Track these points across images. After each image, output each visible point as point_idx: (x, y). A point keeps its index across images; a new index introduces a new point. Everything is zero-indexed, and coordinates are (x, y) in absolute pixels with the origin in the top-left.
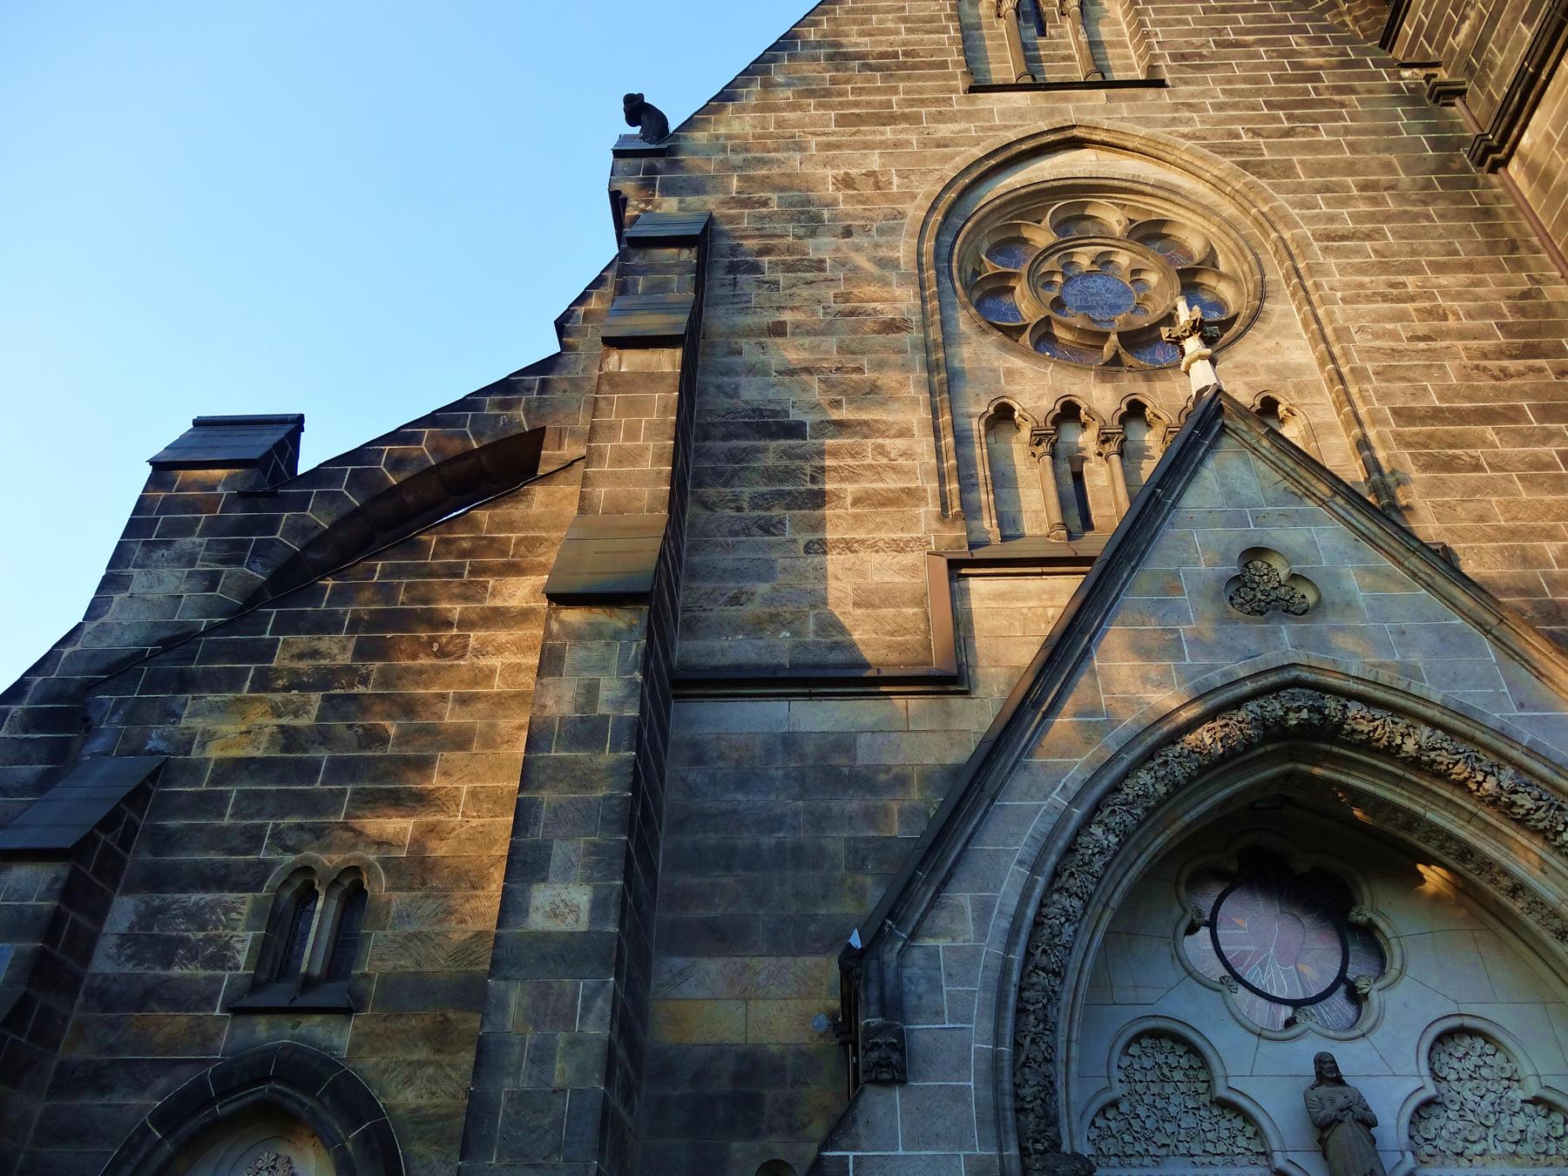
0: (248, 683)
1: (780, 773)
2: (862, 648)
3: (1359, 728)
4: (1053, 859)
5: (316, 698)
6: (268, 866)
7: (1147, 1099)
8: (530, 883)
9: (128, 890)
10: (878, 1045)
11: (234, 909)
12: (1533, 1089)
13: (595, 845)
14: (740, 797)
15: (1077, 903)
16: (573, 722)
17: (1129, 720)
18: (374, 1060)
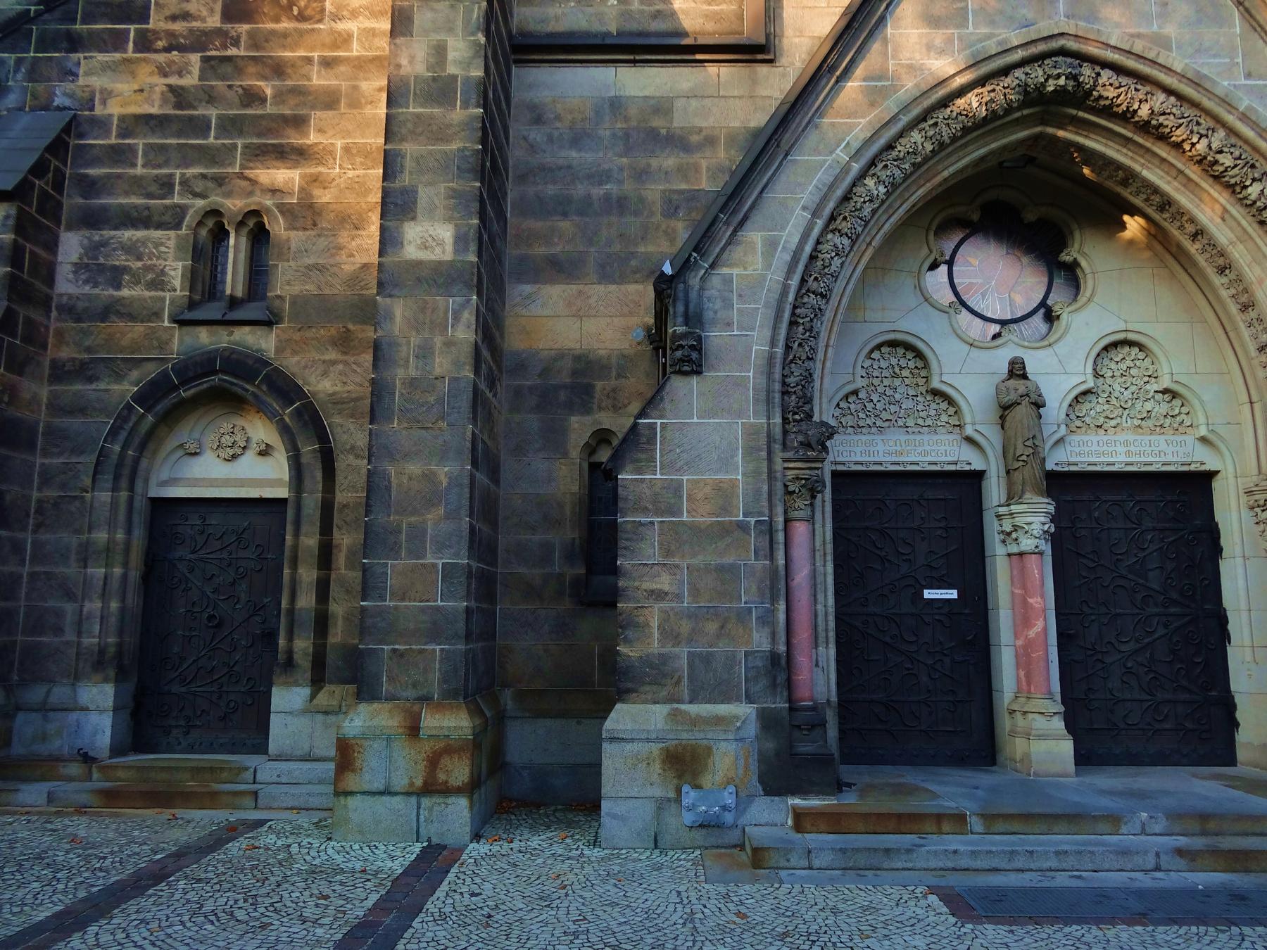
0: (131, 44)
1: (608, 133)
2: (681, 16)
3: (1105, 94)
4: (831, 205)
5: (195, 58)
6: (181, 211)
7: (880, 389)
8: (402, 221)
9: (69, 228)
10: (682, 347)
11: (162, 244)
12: (1166, 383)
13: (453, 190)
14: (574, 154)
15: (846, 241)
16: (425, 80)
17: (909, 86)
18: (296, 359)
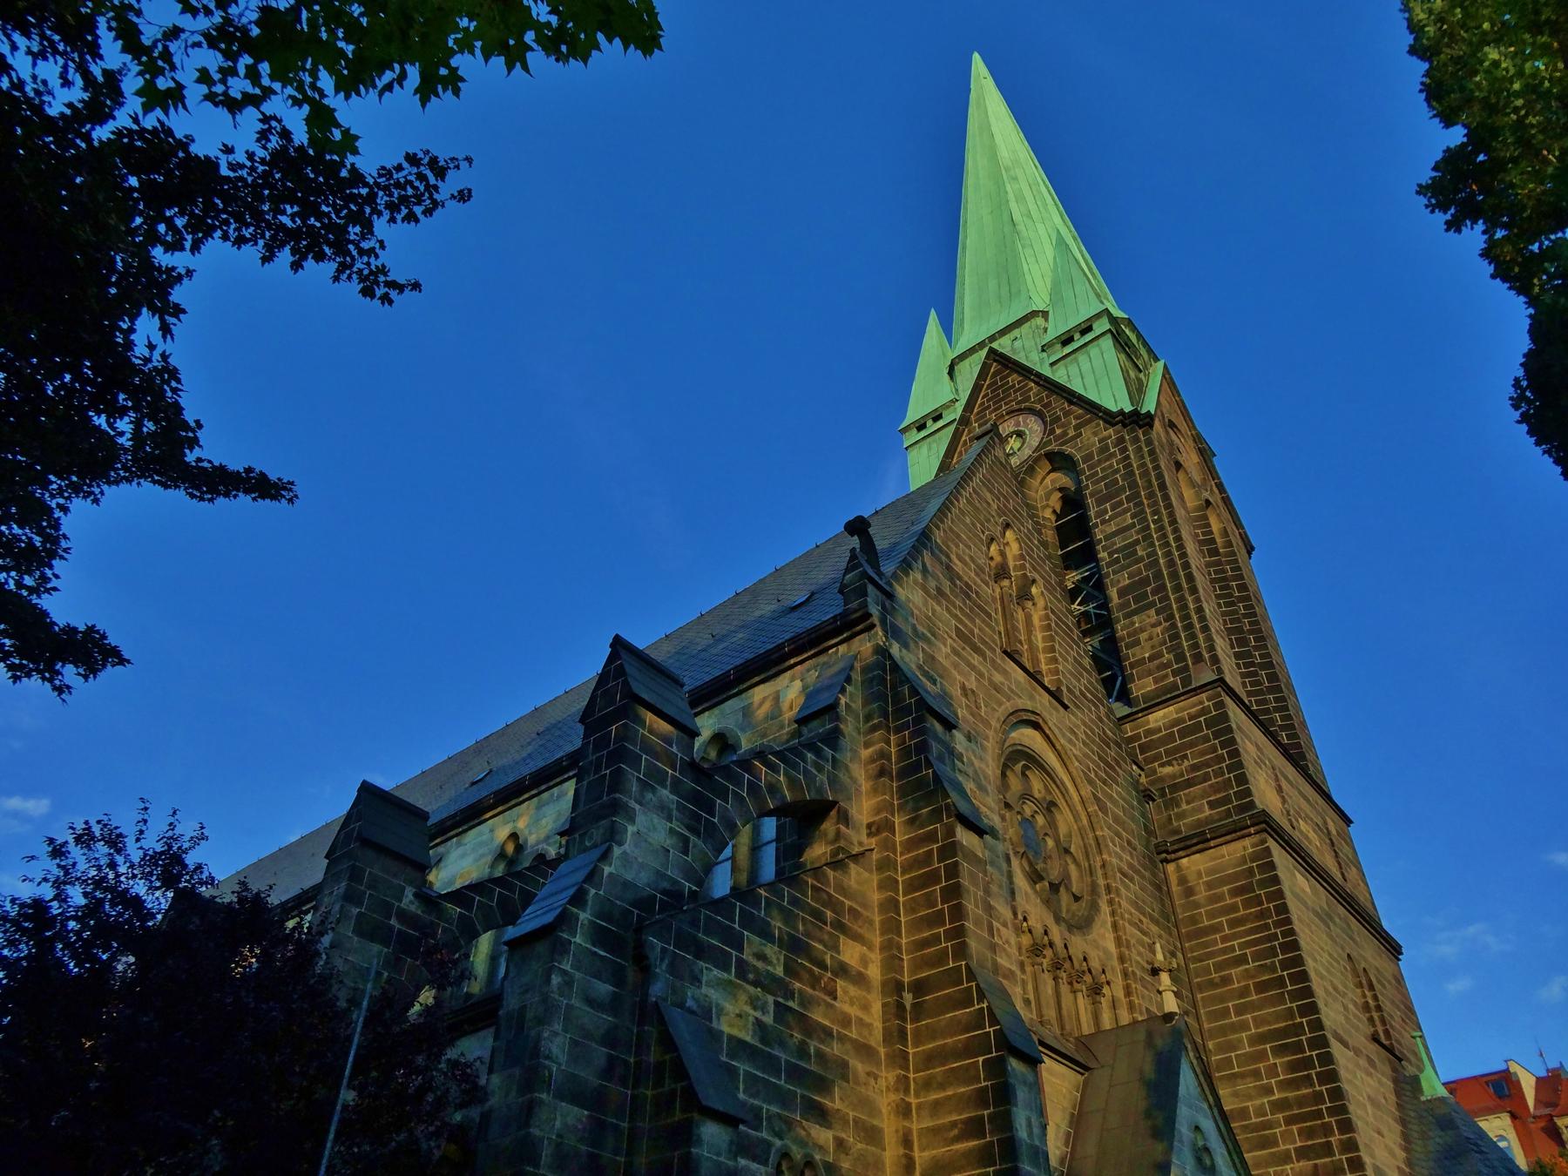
5: (770, 999)
